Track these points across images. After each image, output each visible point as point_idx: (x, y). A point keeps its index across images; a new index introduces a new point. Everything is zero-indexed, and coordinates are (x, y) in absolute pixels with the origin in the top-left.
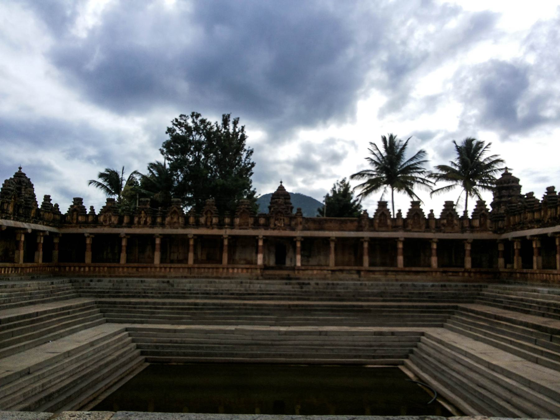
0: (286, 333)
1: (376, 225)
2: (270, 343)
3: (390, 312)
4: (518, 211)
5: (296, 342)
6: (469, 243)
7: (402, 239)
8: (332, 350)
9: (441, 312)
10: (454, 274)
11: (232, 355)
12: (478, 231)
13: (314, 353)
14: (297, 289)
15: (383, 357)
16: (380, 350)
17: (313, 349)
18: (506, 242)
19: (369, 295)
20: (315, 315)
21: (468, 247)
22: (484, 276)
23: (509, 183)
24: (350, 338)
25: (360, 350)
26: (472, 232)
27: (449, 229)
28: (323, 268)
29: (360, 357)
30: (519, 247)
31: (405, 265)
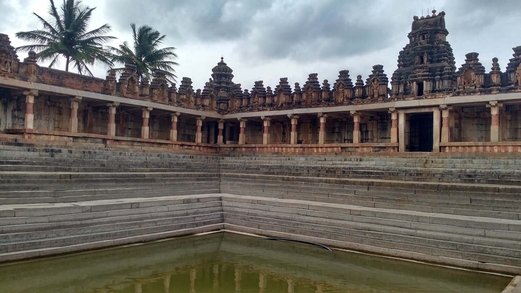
0: (91, 209)
1: (125, 91)
2: (79, 223)
3: (172, 180)
4: (245, 96)
5: (114, 219)
6: (201, 119)
7: (151, 109)
8: (155, 222)
9: (211, 180)
10: (189, 148)
11: (34, 245)
12: (208, 109)
13: (137, 228)
14: (46, 156)
15: (205, 224)
16: (198, 216)
17: (135, 224)
18: (226, 122)
19: (135, 165)
20: (95, 187)
21: (200, 124)
22: (209, 150)
23: (226, 72)
24: (159, 209)
25: (181, 219)
26: (204, 110)
27: (186, 105)
28: (63, 133)
29: (185, 226)
30: (244, 127)
31: (151, 135)
